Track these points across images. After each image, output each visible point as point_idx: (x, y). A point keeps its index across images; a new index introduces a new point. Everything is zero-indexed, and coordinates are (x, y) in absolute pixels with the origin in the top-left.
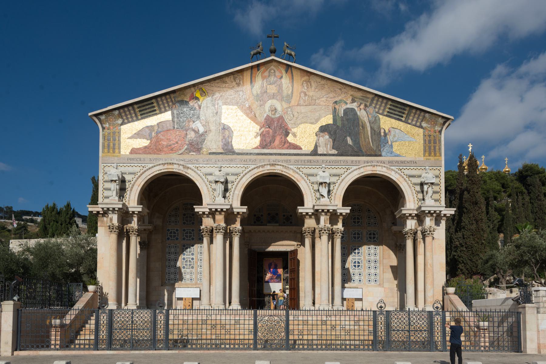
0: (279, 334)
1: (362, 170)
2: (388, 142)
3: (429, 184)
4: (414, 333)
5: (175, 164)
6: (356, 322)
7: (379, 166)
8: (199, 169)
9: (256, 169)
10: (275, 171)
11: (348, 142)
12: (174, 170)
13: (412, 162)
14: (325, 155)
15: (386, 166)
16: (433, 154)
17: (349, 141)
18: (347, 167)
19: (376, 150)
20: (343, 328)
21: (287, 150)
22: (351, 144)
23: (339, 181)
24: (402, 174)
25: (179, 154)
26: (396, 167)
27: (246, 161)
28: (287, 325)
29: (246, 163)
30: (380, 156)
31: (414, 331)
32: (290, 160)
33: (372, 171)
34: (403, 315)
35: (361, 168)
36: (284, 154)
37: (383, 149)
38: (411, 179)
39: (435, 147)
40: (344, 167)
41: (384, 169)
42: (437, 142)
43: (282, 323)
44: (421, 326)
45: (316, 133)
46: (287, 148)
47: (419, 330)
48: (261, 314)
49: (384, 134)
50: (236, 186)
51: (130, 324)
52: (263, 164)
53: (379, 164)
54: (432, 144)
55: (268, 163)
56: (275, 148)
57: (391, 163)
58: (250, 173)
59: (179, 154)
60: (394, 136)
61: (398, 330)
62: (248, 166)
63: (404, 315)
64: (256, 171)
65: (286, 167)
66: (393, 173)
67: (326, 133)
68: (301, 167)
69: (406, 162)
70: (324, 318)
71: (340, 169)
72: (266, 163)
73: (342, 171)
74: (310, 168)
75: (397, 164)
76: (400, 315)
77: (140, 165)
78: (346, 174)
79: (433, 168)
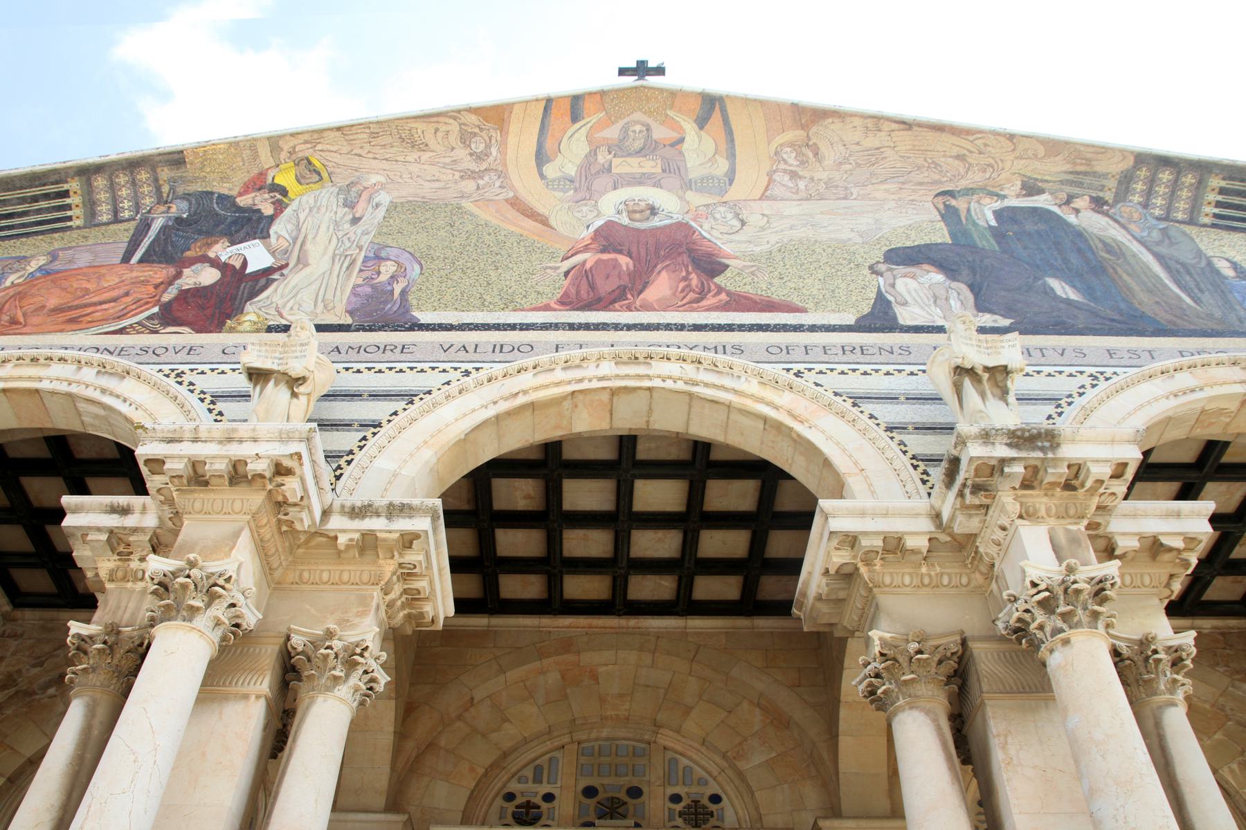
1: (1184, 380)
8: (186, 378)
10: (647, 384)
11: (1059, 292)
12: (45, 385)
22: (1073, 295)
25: (100, 334)
27: (471, 349)
29: (471, 356)
32: (739, 350)
36: (697, 328)
45: (871, 268)
46: (725, 307)
56: (647, 307)
59: (100, 334)
64: (527, 380)
67: (926, 267)
68: (810, 370)
74: (865, 373)
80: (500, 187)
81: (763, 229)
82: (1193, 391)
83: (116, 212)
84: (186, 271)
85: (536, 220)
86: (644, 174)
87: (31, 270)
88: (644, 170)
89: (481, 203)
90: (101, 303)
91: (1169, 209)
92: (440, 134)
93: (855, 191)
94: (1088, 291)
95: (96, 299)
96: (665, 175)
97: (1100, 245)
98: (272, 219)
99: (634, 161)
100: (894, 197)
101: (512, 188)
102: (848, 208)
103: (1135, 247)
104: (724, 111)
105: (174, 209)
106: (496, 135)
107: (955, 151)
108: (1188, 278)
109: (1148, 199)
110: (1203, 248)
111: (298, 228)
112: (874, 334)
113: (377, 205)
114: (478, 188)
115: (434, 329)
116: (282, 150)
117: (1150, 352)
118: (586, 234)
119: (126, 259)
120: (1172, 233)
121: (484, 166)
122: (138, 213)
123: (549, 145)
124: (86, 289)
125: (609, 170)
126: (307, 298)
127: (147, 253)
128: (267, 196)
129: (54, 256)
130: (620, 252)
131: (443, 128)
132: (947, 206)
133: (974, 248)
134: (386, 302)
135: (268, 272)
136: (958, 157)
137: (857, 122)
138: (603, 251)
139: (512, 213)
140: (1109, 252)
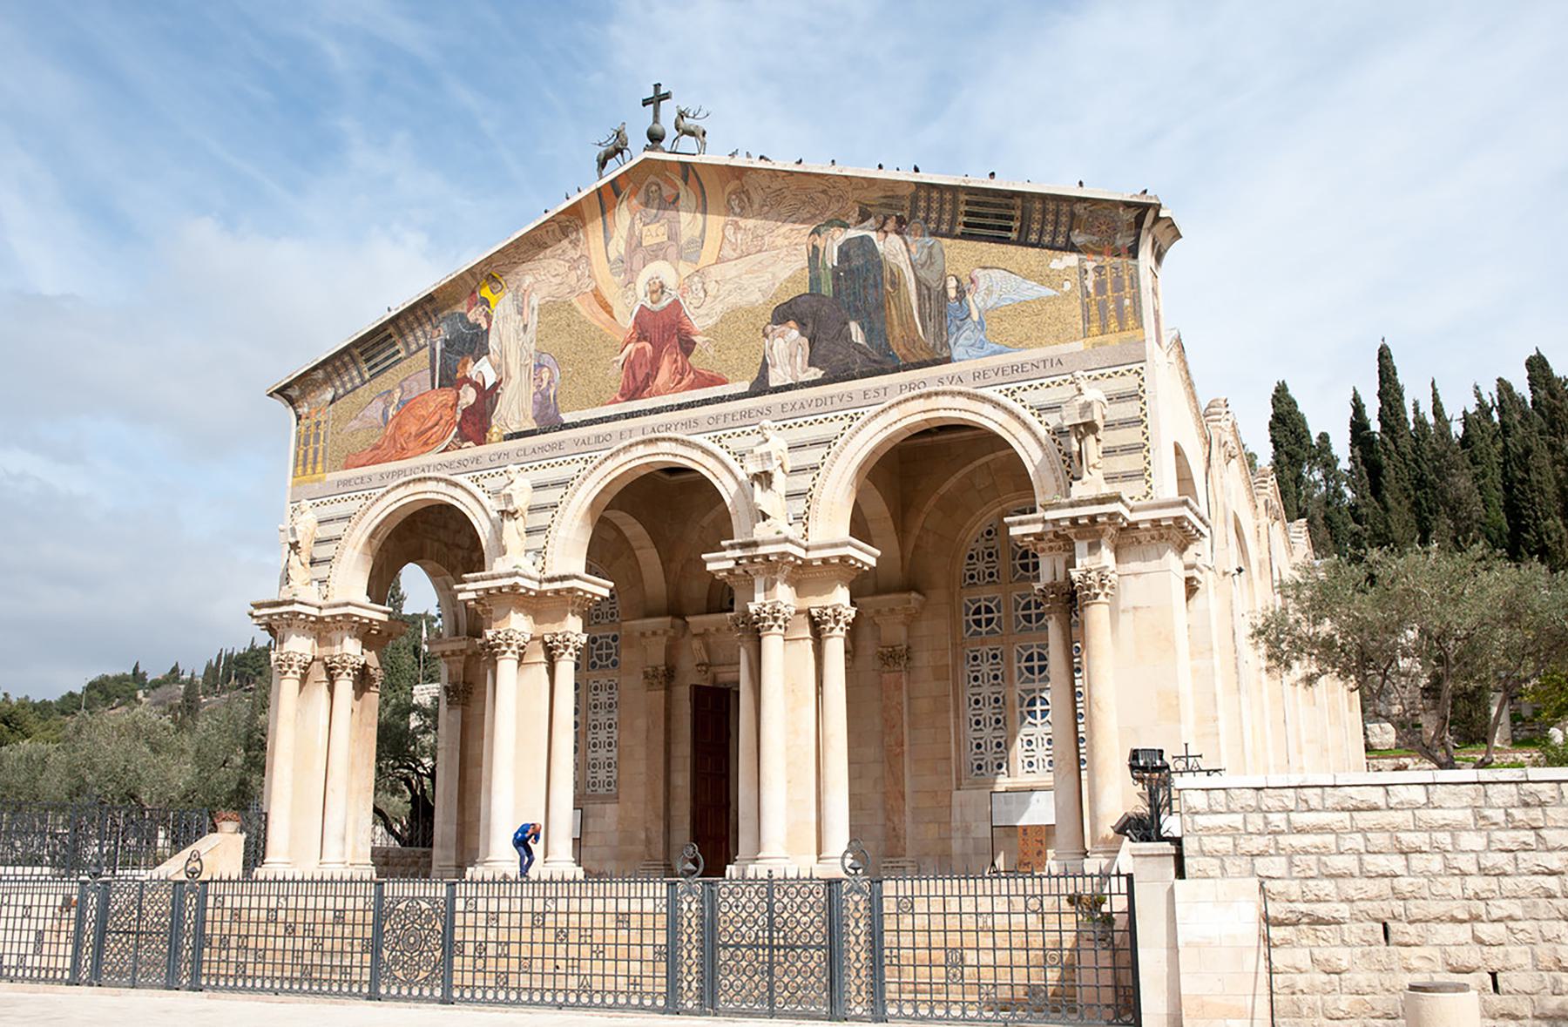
0: (430, 954)
1: (894, 414)
2: (969, 315)
3: (1082, 429)
4: (785, 956)
5: (430, 479)
6: (620, 917)
7: (944, 393)
8: (481, 481)
9: (609, 461)
10: (660, 458)
11: (854, 339)
13: (1048, 364)
14: (788, 388)
15: (963, 388)
16: (1113, 325)
17: (857, 333)
18: (851, 412)
19: (935, 345)
20: (586, 936)
21: (687, 393)
22: (860, 341)
23: (827, 458)
24: (1017, 407)
26: (998, 388)
28: (449, 926)
30: (948, 360)
31: (784, 947)
33: (924, 412)
34: (753, 894)
35: (890, 407)
36: (680, 407)
37: (957, 339)
38: (1045, 418)
39: (1119, 302)
40: (841, 414)
41: (961, 402)
42: (1127, 283)
43: (438, 923)
44: (805, 930)
45: (764, 330)
46: (692, 387)
47: (799, 943)
48: (390, 894)
49: (957, 292)
50: (562, 516)
51: (134, 920)
52: (626, 443)
53: (941, 388)
54: (1110, 294)
55: (639, 438)
57: (981, 377)
58: (595, 473)
60: (989, 292)
61: (737, 946)
62: (590, 454)
63: (756, 893)
64: (610, 464)
65: (683, 441)
66: (987, 409)
67: (792, 323)
69: (1029, 367)
70: (539, 905)
71: (832, 421)
72: (633, 440)
73: (837, 427)
75: (1000, 379)
76: (743, 893)
77: (359, 494)
78: (848, 432)
79: (1115, 369)
80: (589, 276)
81: (715, 297)
82: (895, 422)
83: (417, 340)
84: (461, 391)
85: (607, 312)
86: (658, 244)
87: (396, 401)
88: (658, 240)
89: (580, 297)
90: (431, 428)
91: (939, 222)
92: (550, 233)
93: (766, 238)
94: (869, 332)
95: (430, 424)
96: (670, 243)
97: (889, 276)
98: (487, 331)
99: (653, 227)
100: (786, 242)
101: (595, 280)
102: (760, 263)
103: (909, 275)
104: (694, 170)
105: (442, 332)
106: (579, 223)
107: (821, 188)
108: (927, 306)
109: (928, 215)
110: (947, 265)
111: (500, 339)
112: (756, 399)
113: (533, 309)
114: (578, 281)
115: (570, 428)
116: (475, 273)
117: (885, 389)
118: (630, 322)
119: (433, 388)
120: (935, 250)
121: (579, 254)
122: (426, 338)
123: (608, 220)
124: (423, 416)
125: (641, 243)
126: (514, 407)
127: (440, 379)
128: (481, 309)
129: (401, 386)
130: (645, 339)
131: (549, 229)
132: (814, 247)
133: (819, 294)
134: (548, 407)
135: (496, 385)
136: (824, 192)
137: (764, 172)
138: (639, 340)
139: (596, 307)
140: (893, 284)
